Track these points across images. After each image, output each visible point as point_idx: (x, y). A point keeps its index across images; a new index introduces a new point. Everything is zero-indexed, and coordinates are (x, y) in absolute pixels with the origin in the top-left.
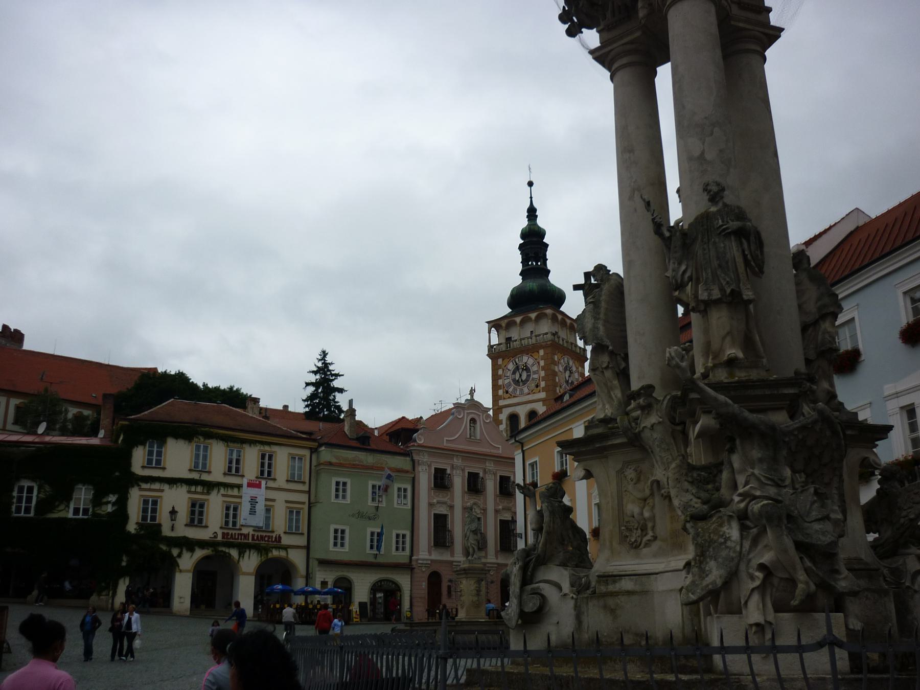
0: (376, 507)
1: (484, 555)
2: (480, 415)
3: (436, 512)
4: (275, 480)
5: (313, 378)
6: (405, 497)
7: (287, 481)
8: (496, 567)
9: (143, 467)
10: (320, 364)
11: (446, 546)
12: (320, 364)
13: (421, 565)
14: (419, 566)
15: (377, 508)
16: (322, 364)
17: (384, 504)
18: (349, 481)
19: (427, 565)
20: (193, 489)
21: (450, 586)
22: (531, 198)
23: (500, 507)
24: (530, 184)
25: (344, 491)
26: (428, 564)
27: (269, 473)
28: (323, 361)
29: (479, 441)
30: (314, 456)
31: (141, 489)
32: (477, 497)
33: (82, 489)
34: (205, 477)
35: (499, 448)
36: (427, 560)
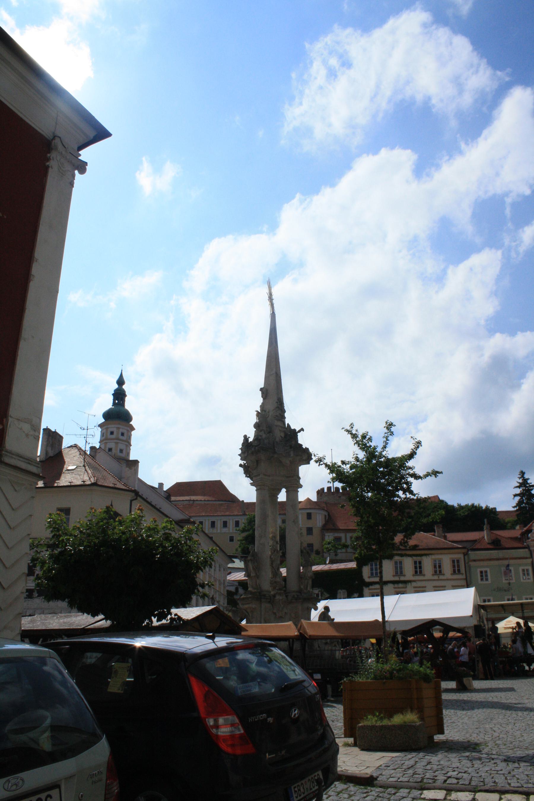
0: (508, 583)
4: (444, 574)
5: (518, 491)
6: (528, 574)
7: (451, 574)
9: (369, 577)
10: (521, 481)
12: (521, 481)
15: (509, 584)
16: (522, 480)
17: (514, 581)
18: (488, 570)
20: (396, 586)
25: (486, 576)
27: (440, 572)
28: (522, 478)
30: (466, 557)
31: (369, 589)
33: (341, 592)
34: (402, 578)
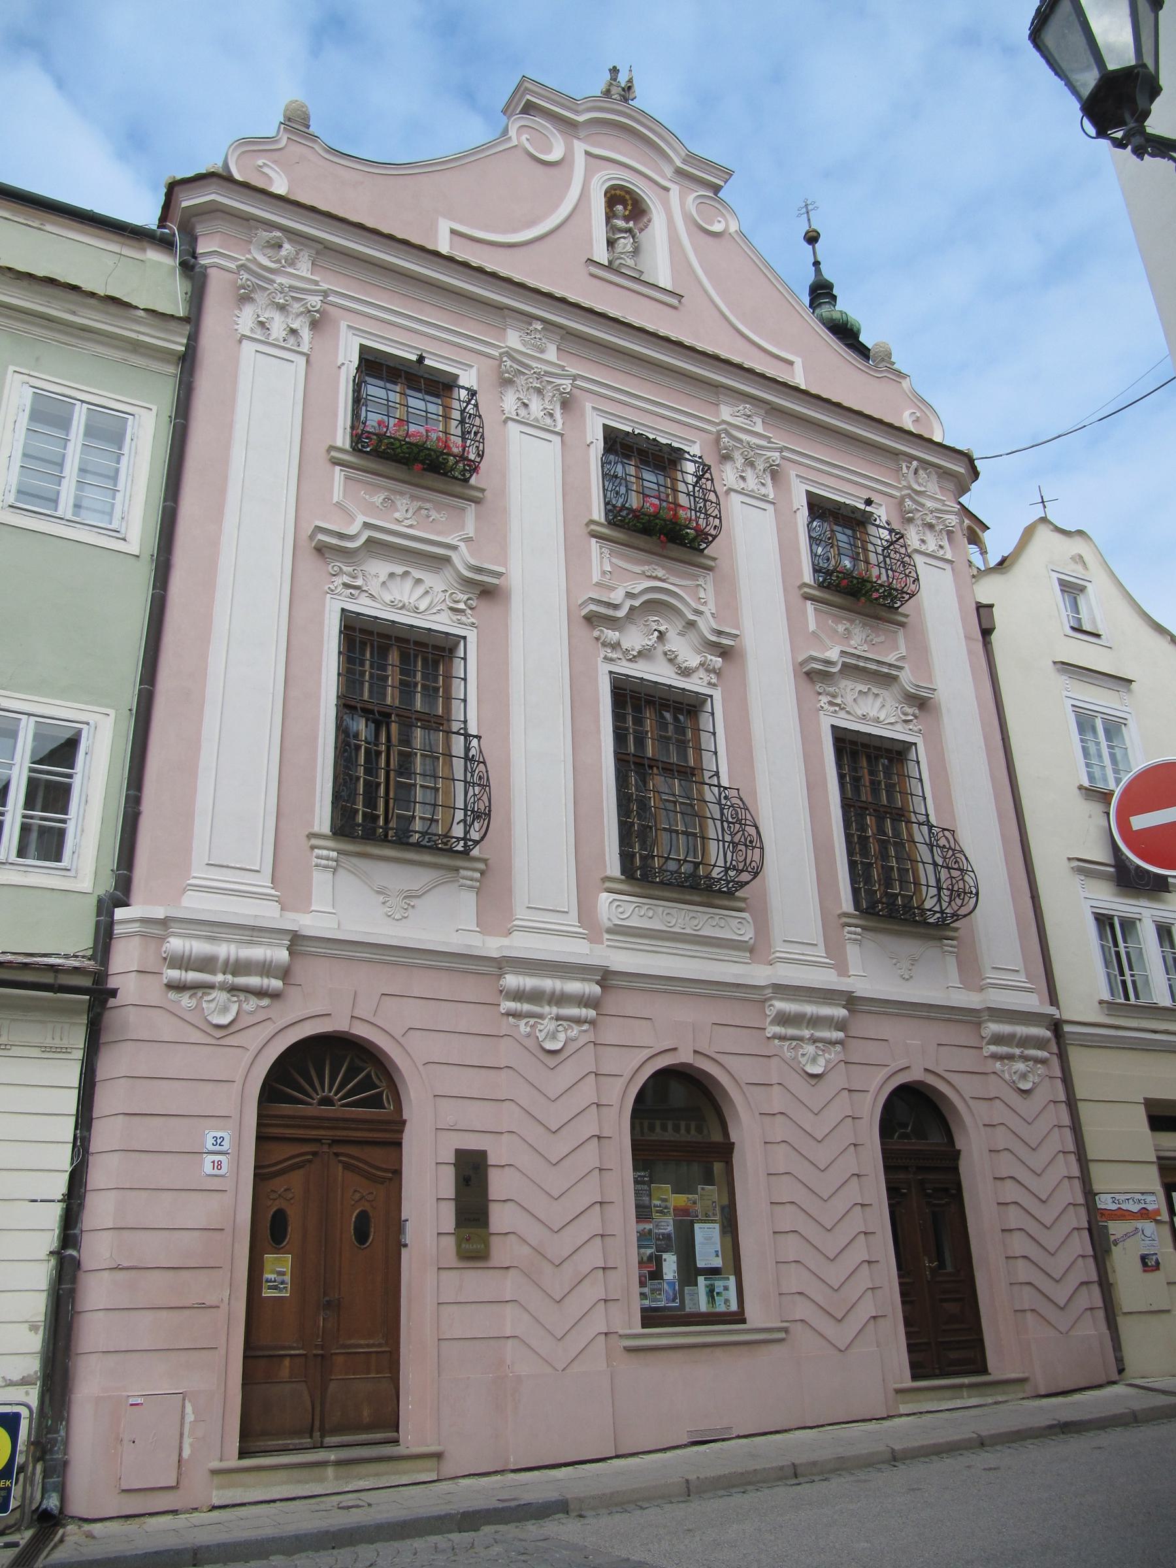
1: (747, 934)
2: (667, 189)
3: (364, 606)
8: (841, 1025)
11: (451, 852)
13: (192, 976)
14: (178, 987)
19: (254, 981)
21: (483, 1154)
22: (816, 264)
23: (833, 654)
24: (812, 238)
26: (265, 969)
29: (674, 302)
32: (669, 570)
35: (791, 363)
36: (253, 932)
